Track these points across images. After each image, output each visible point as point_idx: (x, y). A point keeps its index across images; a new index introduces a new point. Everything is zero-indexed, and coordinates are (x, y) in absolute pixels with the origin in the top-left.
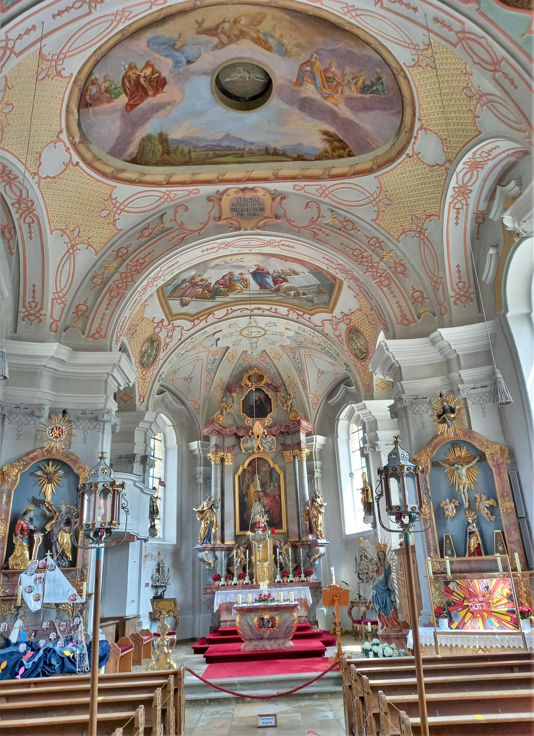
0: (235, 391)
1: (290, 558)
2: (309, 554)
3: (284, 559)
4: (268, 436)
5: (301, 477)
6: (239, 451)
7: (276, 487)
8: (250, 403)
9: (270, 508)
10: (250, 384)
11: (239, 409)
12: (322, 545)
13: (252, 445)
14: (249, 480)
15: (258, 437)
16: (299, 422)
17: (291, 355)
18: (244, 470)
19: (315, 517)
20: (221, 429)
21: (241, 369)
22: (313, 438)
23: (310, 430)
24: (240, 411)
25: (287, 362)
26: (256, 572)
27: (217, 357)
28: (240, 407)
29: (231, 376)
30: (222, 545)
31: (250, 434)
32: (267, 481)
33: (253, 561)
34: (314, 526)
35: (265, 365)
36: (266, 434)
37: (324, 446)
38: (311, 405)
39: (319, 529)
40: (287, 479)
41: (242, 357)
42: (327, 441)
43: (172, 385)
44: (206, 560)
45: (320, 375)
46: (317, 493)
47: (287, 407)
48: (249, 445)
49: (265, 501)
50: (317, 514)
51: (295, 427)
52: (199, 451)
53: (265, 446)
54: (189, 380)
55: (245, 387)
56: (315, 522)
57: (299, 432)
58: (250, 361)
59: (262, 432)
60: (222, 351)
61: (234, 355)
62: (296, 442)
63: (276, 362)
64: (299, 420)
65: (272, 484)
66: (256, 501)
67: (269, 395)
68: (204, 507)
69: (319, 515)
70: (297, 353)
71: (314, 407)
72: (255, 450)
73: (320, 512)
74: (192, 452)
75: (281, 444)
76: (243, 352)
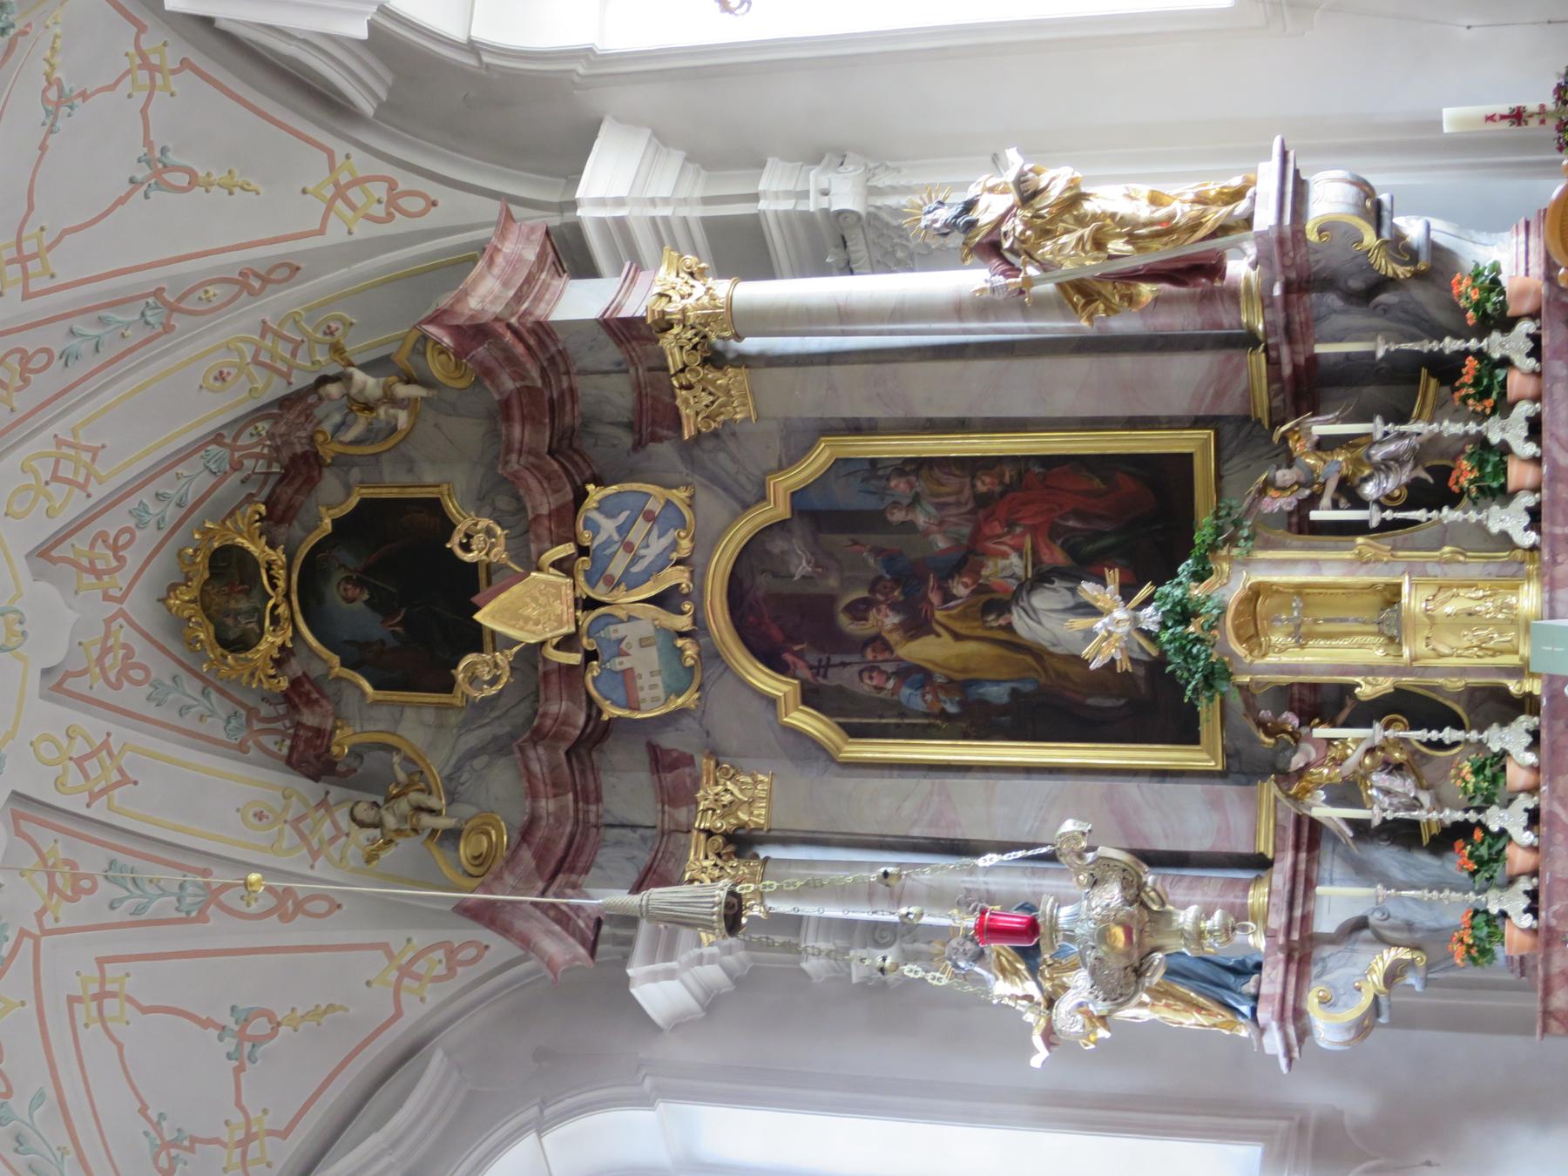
0: (319, 732)
1: (1377, 427)
2: (1356, 284)
3: (1385, 467)
4: (586, 537)
5: (843, 317)
6: (686, 722)
7: (920, 486)
8: (392, 643)
9: (1054, 533)
10: (271, 641)
11: (429, 716)
12: (1297, 193)
13: (644, 643)
14: (872, 669)
15: (589, 604)
16: (477, 332)
17: (44, 384)
18: (811, 697)
19: (1099, 244)
20: (540, 858)
21: (192, 686)
22: (601, 222)
23: (531, 255)
24: (439, 707)
25: (108, 397)
26: (1463, 671)
27: (92, 859)
28: (420, 706)
29: (242, 748)
30: (1280, 876)
31: (575, 658)
32: (877, 552)
33: (1385, 685)
34: (1160, 253)
35: (148, 538)
36: (567, 549)
37: (662, 139)
38: (400, 225)
39: (1182, 210)
40: (864, 411)
41: (100, 690)
42: (630, 120)
43: (284, 1134)
44: (1366, 1000)
45: (181, 179)
46: (944, 215)
47: (390, 399)
48: (645, 663)
49: (1008, 565)
50: (1081, 221)
51: (511, 360)
52: (700, 960)
53: (650, 554)
54: (260, 1026)
55: (295, 667)
56: (1132, 238)
57: (544, 331)
58: (125, 634)
59: (554, 577)
60: (45, 838)
61: (79, 748)
62: (611, 353)
63: (113, 473)
64: (457, 331)
65: (898, 516)
66: (1009, 628)
67: (339, 512)
68: (1029, 998)
69: (1088, 207)
70: (29, 341)
71: (417, 204)
72: (683, 622)
73: (1074, 200)
74: (712, 1003)
75: (638, 445)
76: (58, 687)
